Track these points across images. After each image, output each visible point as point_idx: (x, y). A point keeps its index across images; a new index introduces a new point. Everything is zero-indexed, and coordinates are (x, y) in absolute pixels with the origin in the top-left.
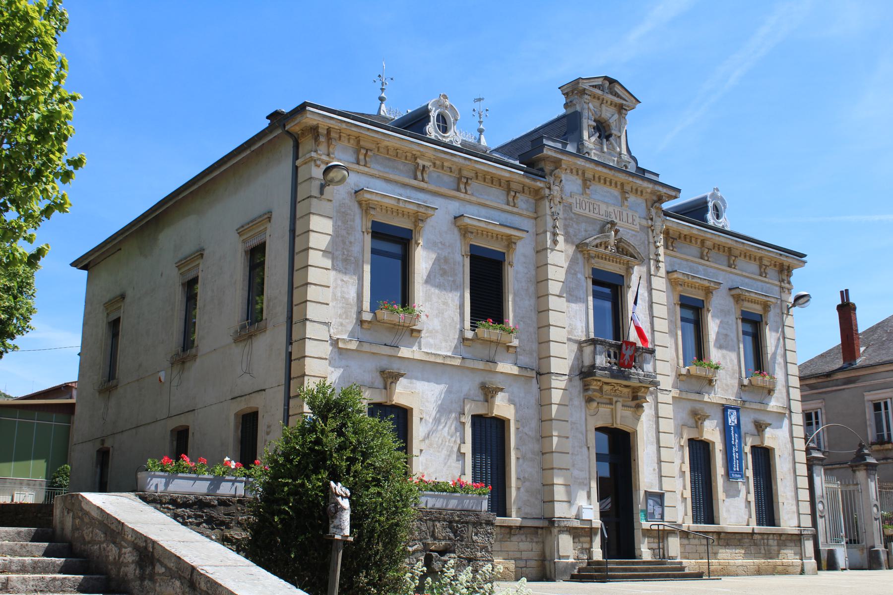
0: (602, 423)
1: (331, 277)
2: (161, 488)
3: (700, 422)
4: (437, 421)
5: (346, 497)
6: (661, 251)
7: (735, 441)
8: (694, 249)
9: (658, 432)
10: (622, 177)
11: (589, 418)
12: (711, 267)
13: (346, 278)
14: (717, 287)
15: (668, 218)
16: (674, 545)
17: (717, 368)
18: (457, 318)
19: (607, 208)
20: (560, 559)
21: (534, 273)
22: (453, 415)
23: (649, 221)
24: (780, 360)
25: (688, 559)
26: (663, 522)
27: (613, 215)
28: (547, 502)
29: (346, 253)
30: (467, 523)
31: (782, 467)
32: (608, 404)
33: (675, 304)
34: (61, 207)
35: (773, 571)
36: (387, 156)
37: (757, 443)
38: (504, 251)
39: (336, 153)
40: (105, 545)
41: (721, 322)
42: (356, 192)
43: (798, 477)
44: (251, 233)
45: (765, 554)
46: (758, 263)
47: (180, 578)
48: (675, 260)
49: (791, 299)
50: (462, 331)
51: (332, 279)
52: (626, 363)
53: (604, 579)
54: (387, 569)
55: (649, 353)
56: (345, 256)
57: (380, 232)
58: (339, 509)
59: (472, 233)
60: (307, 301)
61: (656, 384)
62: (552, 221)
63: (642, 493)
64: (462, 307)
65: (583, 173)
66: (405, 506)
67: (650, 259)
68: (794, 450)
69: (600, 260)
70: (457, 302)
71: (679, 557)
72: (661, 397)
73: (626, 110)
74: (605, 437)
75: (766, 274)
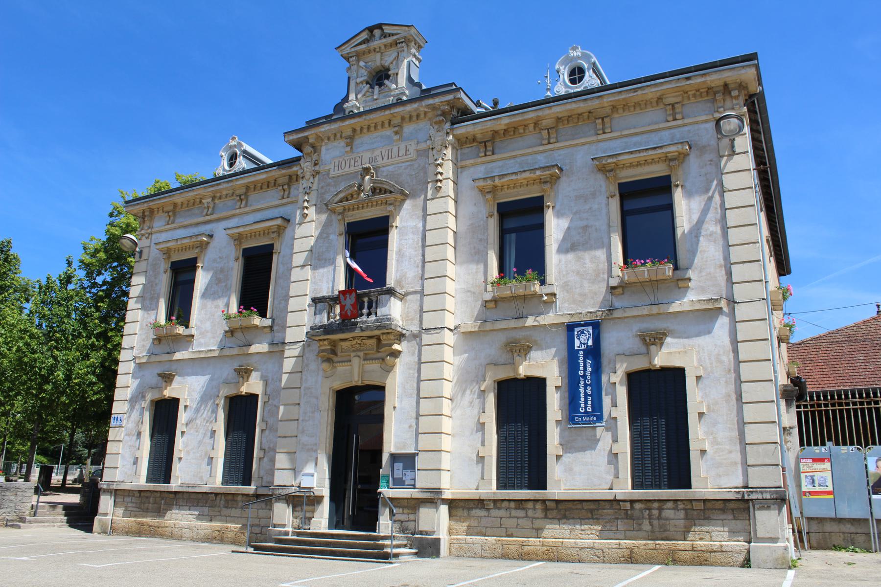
12: (559, 148)
15: (456, 126)
25: (485, 535)
29: (152, 292)
52: (349, 313)
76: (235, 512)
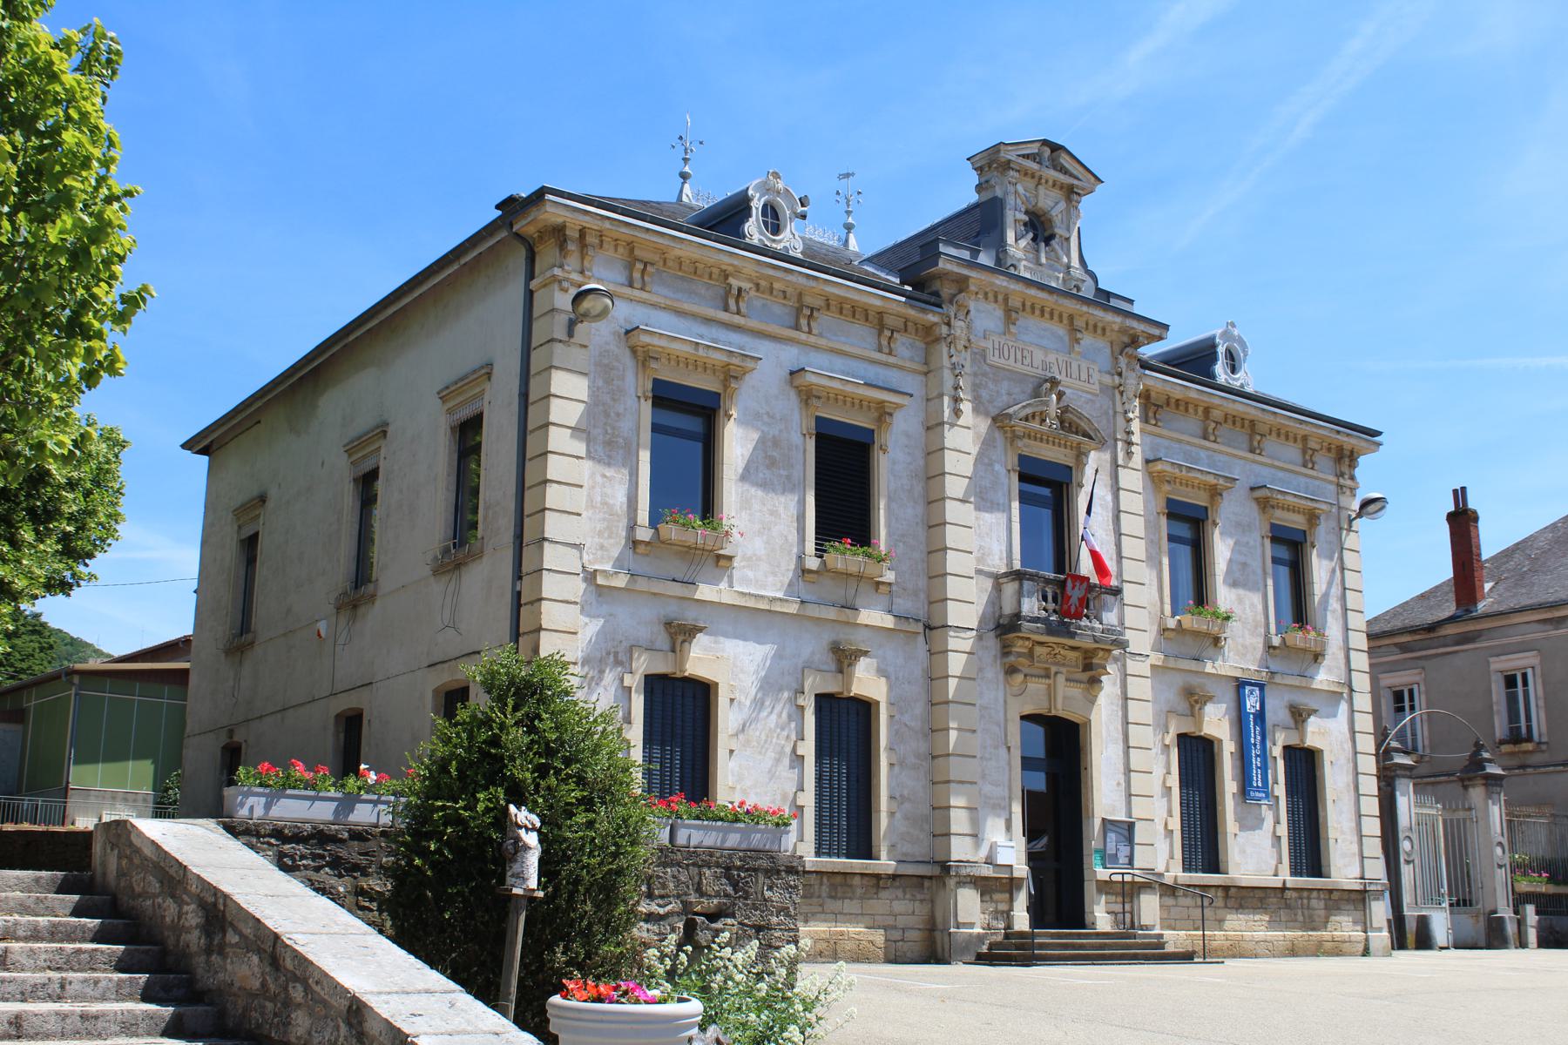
0: (1032, 707)
1: (585, 471)
2: (259, 812)
3: (1197, 707)
4: (758, 704)
5: (534, 829)
6: (1136, 426)
7: (1255, 738)
8: (1193, 423)
9: (1126, 722)
10: (1069, 305)
11: (1010, 700)
12: (1221, 452)
13: (609, 472)
14: (1229, 485)
15: (1147, 372)
16: (1150, 908)
17: (1228, 618)
18: (793, 537)
19: (1046, 356)
20: (958, 928)
21: (921, 462)
22: (786, 695)
23: (1116, 377)
24: (1334, 604)
25: (1174, 929)
26: (1133, 869)
27: (1055, 369)
28: (939, 835)
29: (609, 431)
30: (755, 870)
31: (1335, 781)
32: (1042, 677)
33: (1158, 513)
34: (112, 370)
35: (1318, 950)
36: (680, 274)
37: (1294, 741)
38: (872, 427)
39: (595, 269)
40: (160, 900)
41: (1235, 543)
42: (627, 332)
43: (1361, 797)
44: (461, 399)
45: (1304, 922)
46: (1301, 446)
47: (259, 951)
48: (1159, 440)
49: (1356, 505)
50: (800, 558)
51: (586, 474)
52: (1073, 611)
53: (1027, 961)
54: (600, 941)
55: (1111, 594)
56: (608, 436)
57: (666, 398)
58: (520, 848)
59: (819, 398)
60: (545, 509)
61: (1123, 645)
62: (952, 377)
63: (1097, 823)
64: (801, 518)
65: (1006, 299)
66: (633, 843)
67: (1116, 440)
68: (1356, 753)
69: (1032, 442)
70: (793, 511)
71: (1158, 926)
72: (1133, 666)
73: (1079, 194)
74: (1039, 732)
75: (1313, 463)
76: (850, 906)
